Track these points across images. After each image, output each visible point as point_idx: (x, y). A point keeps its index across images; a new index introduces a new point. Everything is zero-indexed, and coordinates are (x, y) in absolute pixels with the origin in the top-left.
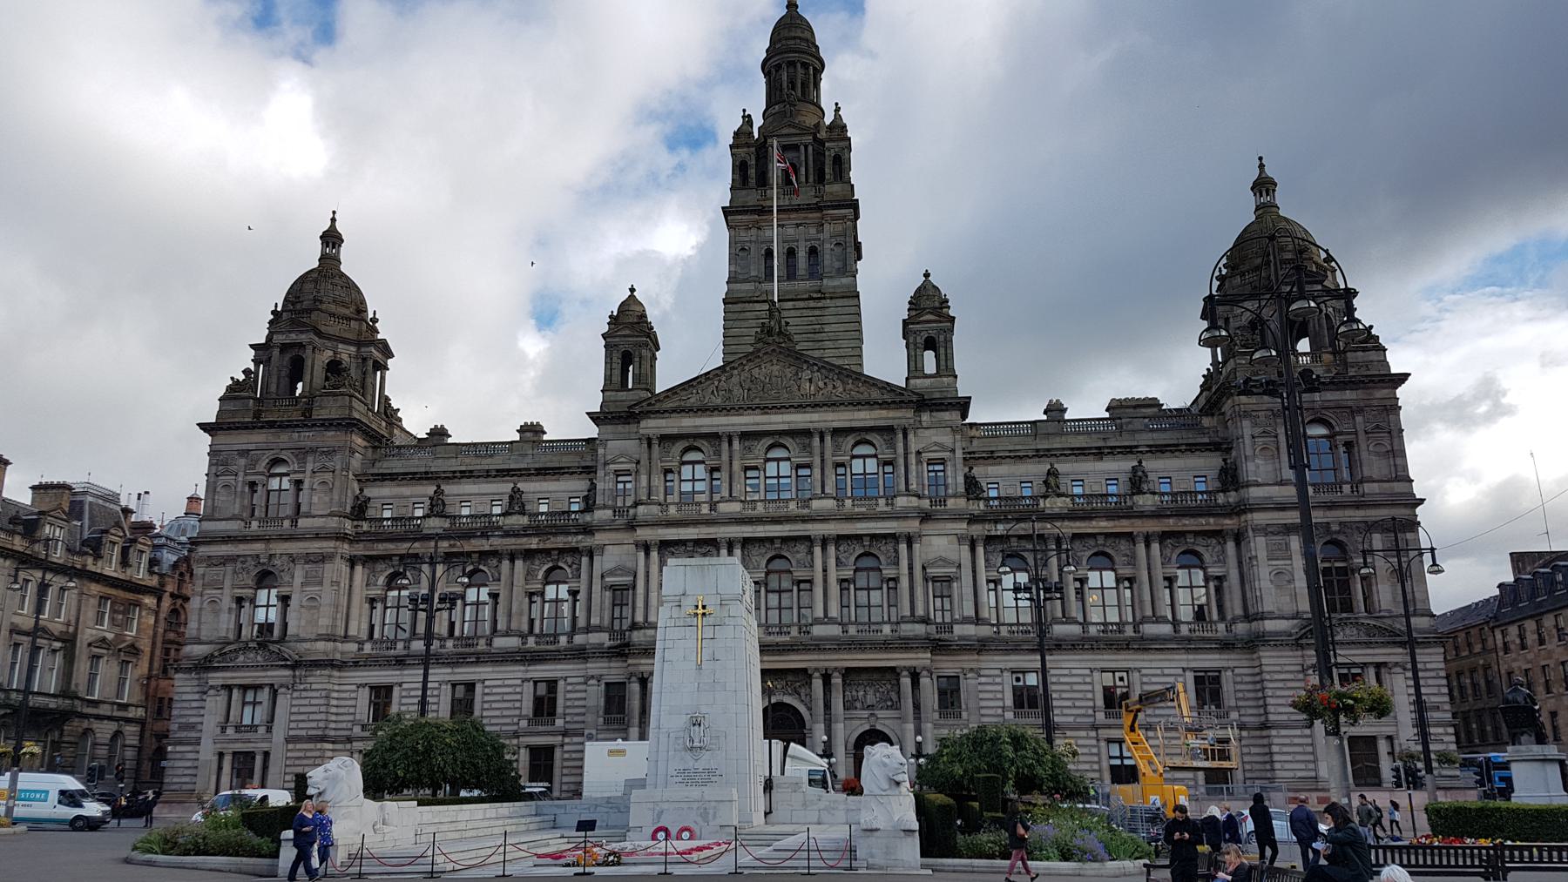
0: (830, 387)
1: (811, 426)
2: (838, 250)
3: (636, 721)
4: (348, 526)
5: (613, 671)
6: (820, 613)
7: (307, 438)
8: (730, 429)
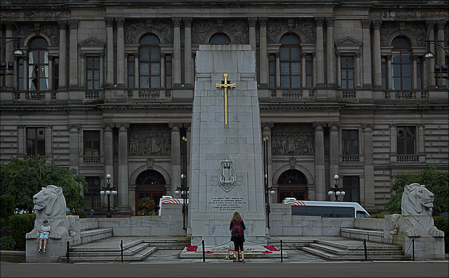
3: (111, 160)
5: (91, 122)
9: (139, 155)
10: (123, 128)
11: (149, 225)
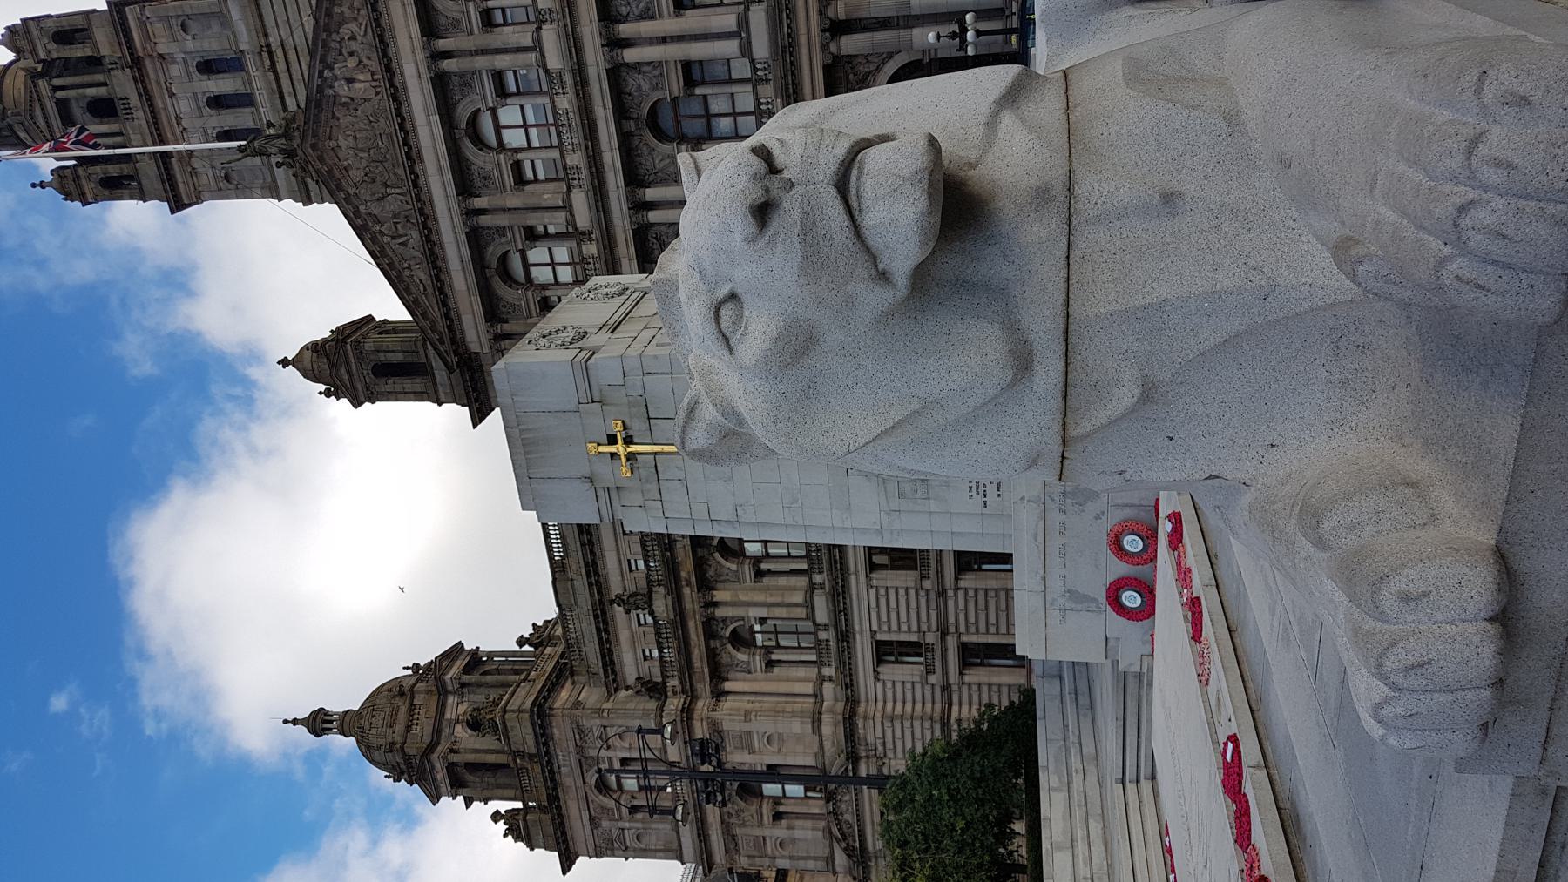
0: (354, 46)
1: (425, 76)
2: (194, 27)
4: (674, 704)
6: (731, 47)
7: (565, 758)
8: (456, 213)
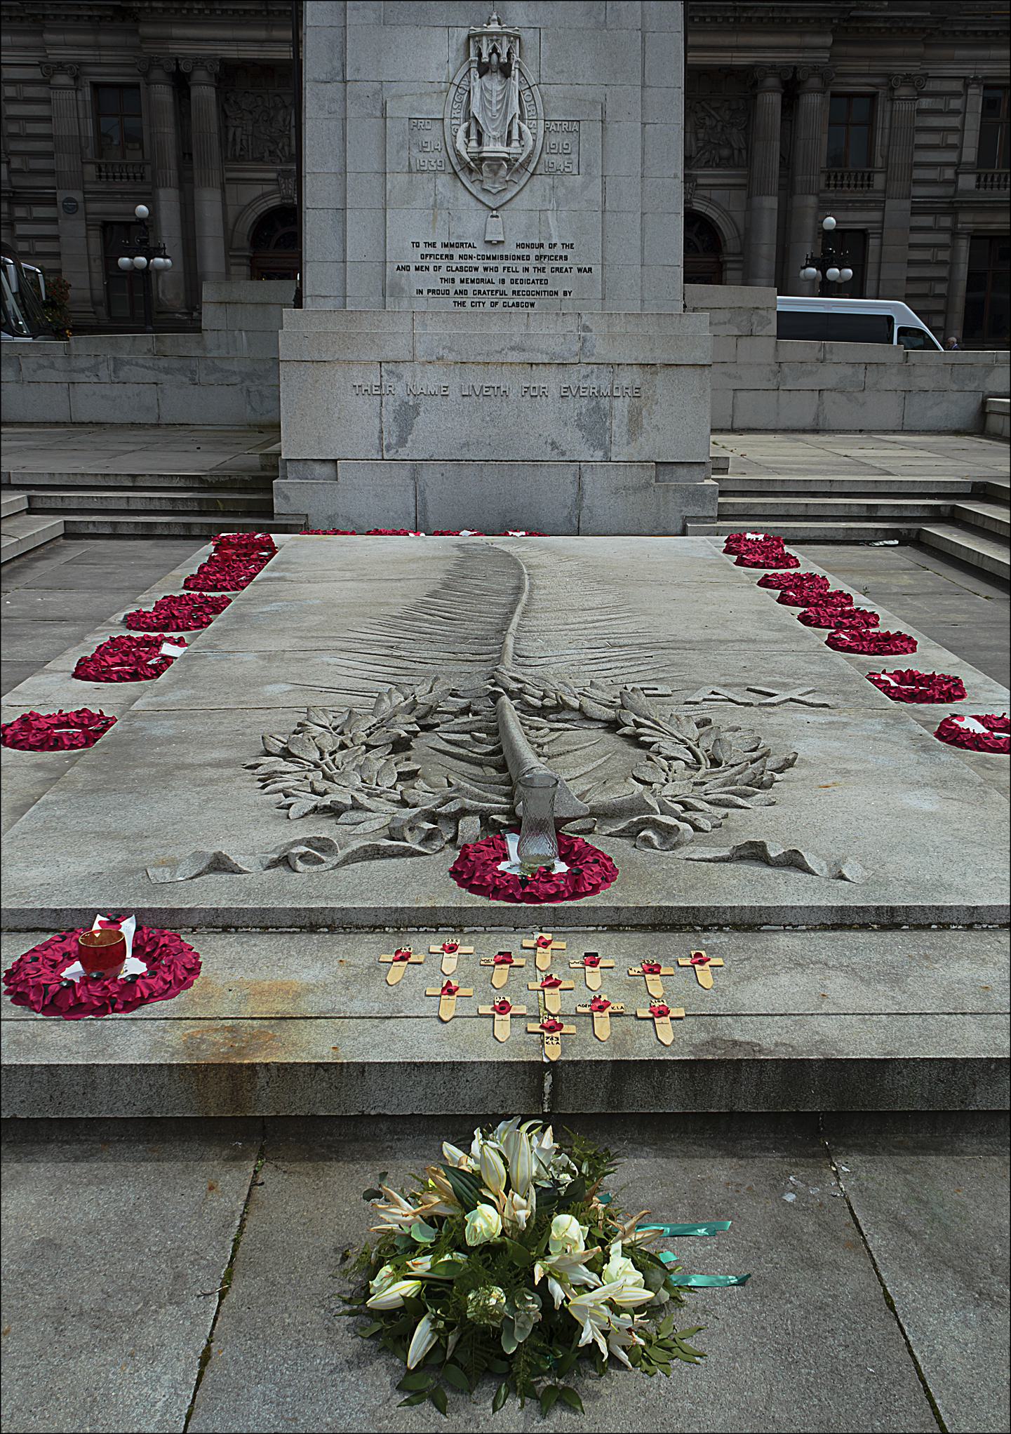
3: (172, 173)
9: (254, 160)
10: (200, 75)
11: (150, 376)
